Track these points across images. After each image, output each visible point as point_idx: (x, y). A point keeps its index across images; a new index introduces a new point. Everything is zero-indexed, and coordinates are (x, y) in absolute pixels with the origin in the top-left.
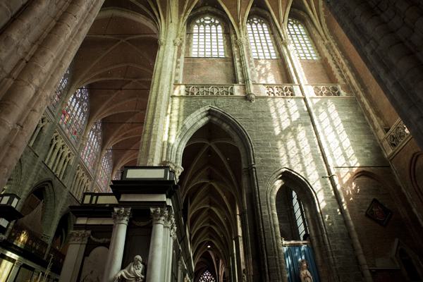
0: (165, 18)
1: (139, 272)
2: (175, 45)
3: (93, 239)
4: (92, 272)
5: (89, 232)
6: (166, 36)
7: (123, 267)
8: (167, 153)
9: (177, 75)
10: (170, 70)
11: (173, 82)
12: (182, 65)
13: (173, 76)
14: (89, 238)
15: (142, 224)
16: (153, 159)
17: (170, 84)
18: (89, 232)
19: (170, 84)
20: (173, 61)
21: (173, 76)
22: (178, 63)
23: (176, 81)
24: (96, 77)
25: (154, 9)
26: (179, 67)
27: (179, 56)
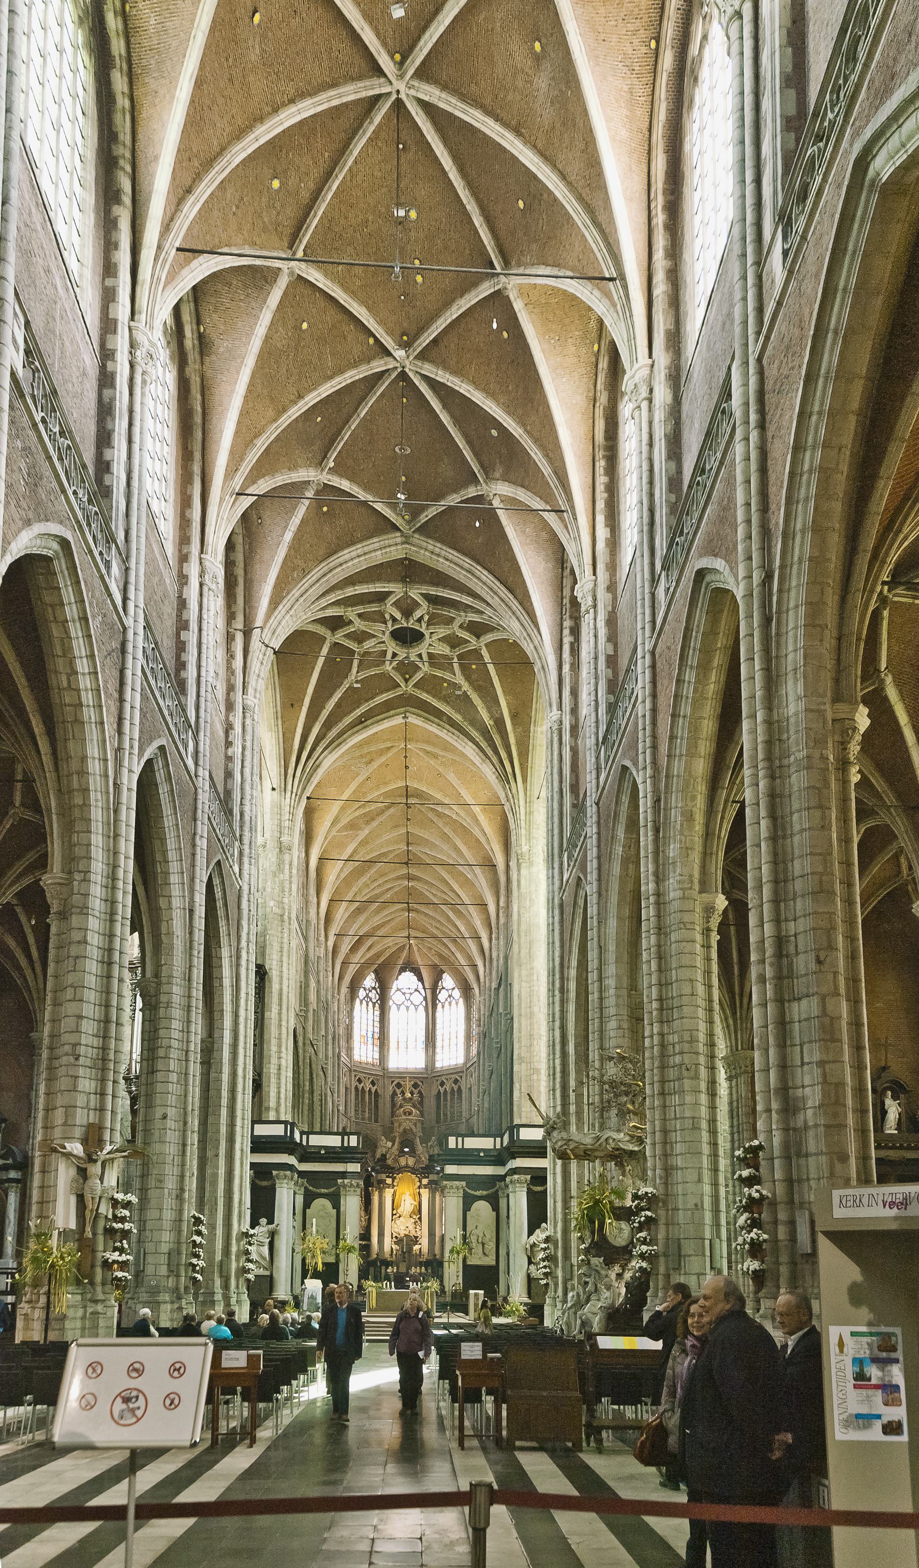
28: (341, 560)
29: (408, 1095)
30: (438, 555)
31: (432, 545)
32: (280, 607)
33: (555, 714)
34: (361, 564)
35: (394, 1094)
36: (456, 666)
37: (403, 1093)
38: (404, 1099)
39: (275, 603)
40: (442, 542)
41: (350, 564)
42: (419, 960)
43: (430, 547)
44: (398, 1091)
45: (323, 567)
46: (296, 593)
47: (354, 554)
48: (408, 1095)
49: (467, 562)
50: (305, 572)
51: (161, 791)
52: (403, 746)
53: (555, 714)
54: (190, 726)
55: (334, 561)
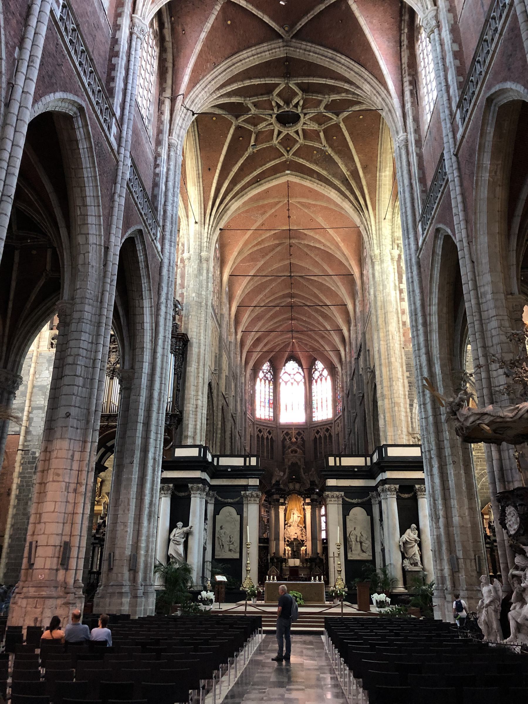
0: (374, 209)
1: (416, 536)
2: (392, 259)
3: (347, 499)
4: (355, 529)
5: (343, 493)
6: (380, 245)
7: (402, 532)
8: (412, 422)
9: (403, 313)
10: (395, 307)
11: (401, 325)
12: (405, 295)
13: (400, 315)
14: (343, 499)
15: (406, 496)
16: (402, 431)
17: (399, 329)
18: (343, 493)
19: (399, 329)
20: (396, 290)
21: (400, 315)
22: (401, 291)
23: (404, 324)
24: (249, 250)
25: (358, 193)
26: (404, 299)
27: (401, 282)
28: (241, 57)
29: (294, 440)
30: (310, 51)
31: (304, 45)
32: (198, 86)
33: (402, 135)
34: (256, 61)
35: (284, 439)
36: (322, 134)
37: (290, 439)
38: (292, 443)
39: (194, 82)
40: (312, 42)
41: (247, 60)
42: (300, 355)
43: (303, 47)
44: (287, 438)
45: (229, 62)
46: (209, 77)
47: (250, 54)
48: (294, 440)
49: (330, 53)
50: (215, 65)
51: (80, 146)
52: (286, 201)
53: (402, 135)
54: (114, 115)
55: (235, 59)
